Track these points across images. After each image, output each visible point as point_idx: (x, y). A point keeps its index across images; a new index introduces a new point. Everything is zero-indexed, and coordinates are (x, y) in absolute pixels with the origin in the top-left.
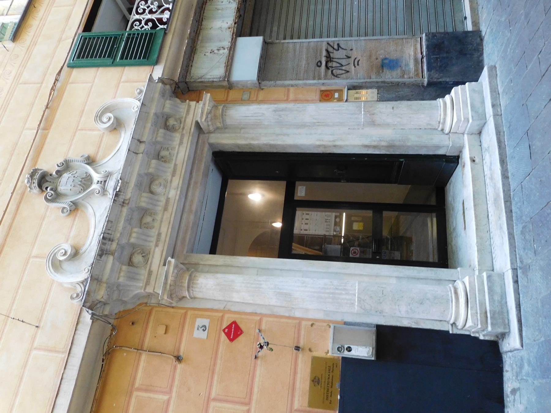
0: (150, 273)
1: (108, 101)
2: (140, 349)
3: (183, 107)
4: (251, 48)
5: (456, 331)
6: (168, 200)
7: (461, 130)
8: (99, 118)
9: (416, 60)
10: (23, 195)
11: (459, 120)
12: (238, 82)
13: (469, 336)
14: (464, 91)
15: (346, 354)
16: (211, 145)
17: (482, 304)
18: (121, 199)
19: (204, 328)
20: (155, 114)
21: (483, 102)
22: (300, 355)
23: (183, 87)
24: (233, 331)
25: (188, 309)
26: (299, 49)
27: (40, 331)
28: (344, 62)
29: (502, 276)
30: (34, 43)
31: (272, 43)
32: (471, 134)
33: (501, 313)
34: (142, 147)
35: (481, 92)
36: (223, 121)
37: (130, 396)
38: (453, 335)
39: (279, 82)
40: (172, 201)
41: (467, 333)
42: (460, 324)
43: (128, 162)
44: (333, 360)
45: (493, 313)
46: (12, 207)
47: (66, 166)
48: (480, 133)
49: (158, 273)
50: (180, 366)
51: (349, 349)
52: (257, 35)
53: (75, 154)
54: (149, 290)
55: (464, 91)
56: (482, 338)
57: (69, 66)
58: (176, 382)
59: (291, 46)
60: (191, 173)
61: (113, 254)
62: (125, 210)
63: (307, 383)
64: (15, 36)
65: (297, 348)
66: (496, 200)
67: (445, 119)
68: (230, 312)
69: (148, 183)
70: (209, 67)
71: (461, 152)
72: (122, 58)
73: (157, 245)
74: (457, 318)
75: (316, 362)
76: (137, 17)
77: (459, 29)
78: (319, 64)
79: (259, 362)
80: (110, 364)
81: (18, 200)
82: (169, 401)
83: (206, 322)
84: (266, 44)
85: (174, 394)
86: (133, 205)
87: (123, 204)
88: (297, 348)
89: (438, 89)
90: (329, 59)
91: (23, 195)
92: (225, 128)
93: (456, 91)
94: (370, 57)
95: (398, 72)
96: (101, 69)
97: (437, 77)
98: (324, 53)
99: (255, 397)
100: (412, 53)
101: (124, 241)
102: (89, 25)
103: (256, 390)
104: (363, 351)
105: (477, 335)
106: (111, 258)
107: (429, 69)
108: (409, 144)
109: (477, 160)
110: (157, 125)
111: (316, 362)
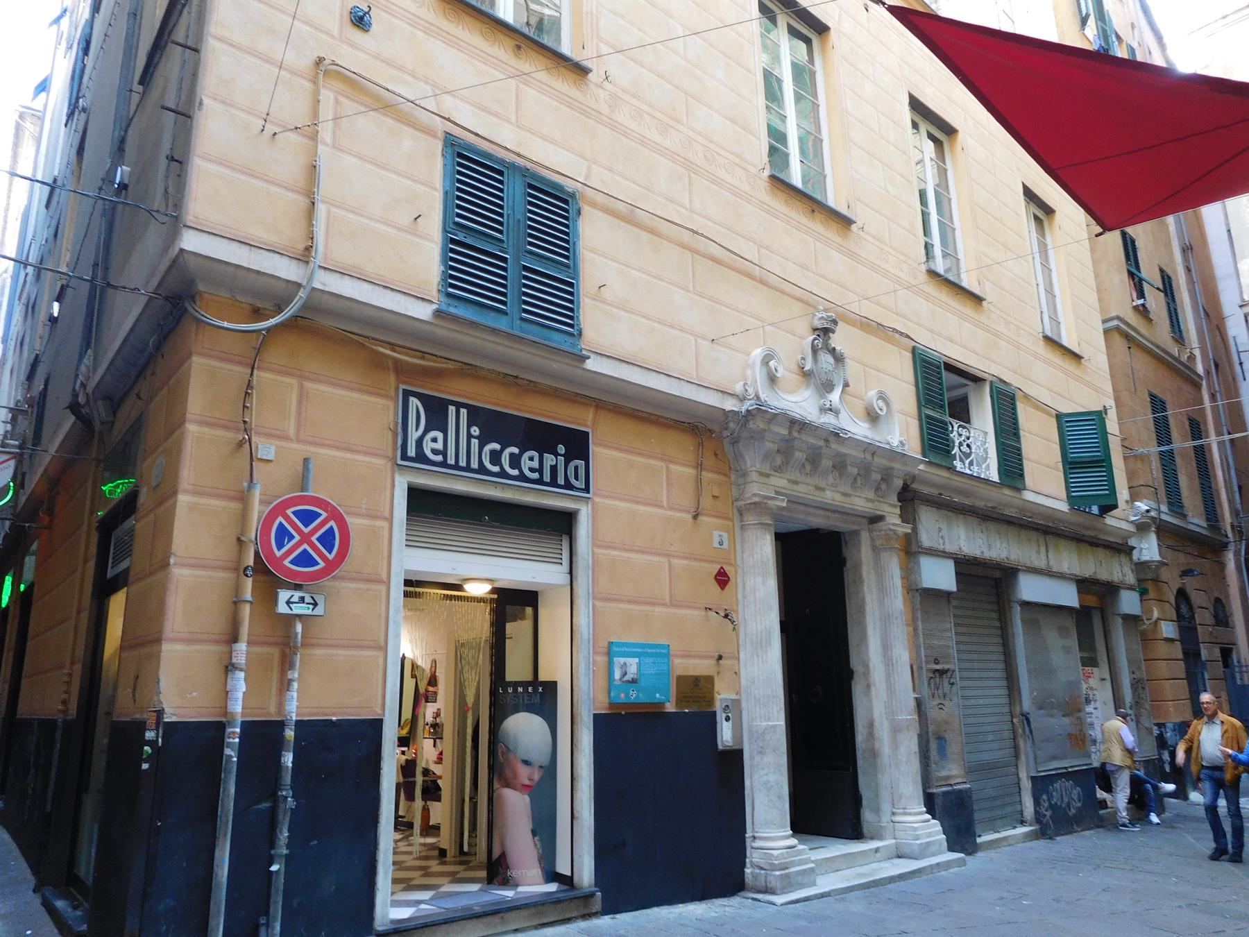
0: (768, 476)
1: (895, 405)
2: (699, 466)
3: (894, 499)
4: (940, 576)
5: (748, 843)
6: (823, 490)
7: (898, 834)
8: (882, 396)
9: (948, 778)
10: (808, 304)
11: (915, 829)
12: (918, 564)
13: (745, 856)
14: (937, 833)
15: (721, 716)
16: (856, 533)
17: (793, 864)
18: (832, 439)
19: (721, 543)
20: (892, 468)
21: (934, 855)
22: (713, 662)
23: (909, 498)
24: (722, 579)
25: (732, 520)
26: (947, 636)
27: (709, 343)
28: (940, 691)
29: (814, 884)
30: (928, 298)
31: (949, 602)
32: (897, 846)
33: (790, 885)
34: (869, 457)
35: (940, 853)
36: (885, 549)
37: (662, 459)
38: (744, 838)
39: (919, 613)
40: (821, 494)
41: (748, 854)
42: (758, 844)
43: (858, 443)
44: (711, 702)
45: (787, 876)
46: (798, 292)
47: (839, 359)
48: (899, 857)
49: (768, 486)
50: (689, 517)
51: (727, 719)
52: (958, 582)
53: (852, 369)
54: (754, 476)
55: (937, 833)
56: (748, 871)
57: (914, 348)
58: (678, 514)
59: (948, 626)
60: (835, 512)
61: (790, 433)
62: (821, 443)
63: (693, 673)
64: (1047, 339)
65: (720, 658)
66: (862, 875)
67: (910, 814)
68: (736, 572)
69: (840, 465)
70: (933, 528)
71: (872, 839)
72: (928, 417)
73: (789, 481)
74: (761, 838)
75: (709, 680)
76: (956, 427)
77: (978, 828)
78: (937, 662)
79: (703, 613)
80: (684, 431)
81: (807, 301)
82: (662, 507)
83: (725, 546)
84: (947, 595)
85: (669, 513)
86: (824, 450)
87: (827, 441)
88: (720, 658)
89: (930, 804)
90: (942, 673)
91: (808, 304)
92: (875, 549)
93: (936, 826)
94: (946, 723)
95: (937, 758)
96: (913, 389)
97: (939, 802)
98: (946, 667)
99: (678, 611)
100: (953, 773)
101: (796, 443)
102: (950, 368)
103: (683, 611)
104: (726, 735)
105: (748, 865)
106: (786, 432)
107: (944, 793)
108: (879, 776)
109: (878, 855)
110: (871, 466)
111: (709, 680)
